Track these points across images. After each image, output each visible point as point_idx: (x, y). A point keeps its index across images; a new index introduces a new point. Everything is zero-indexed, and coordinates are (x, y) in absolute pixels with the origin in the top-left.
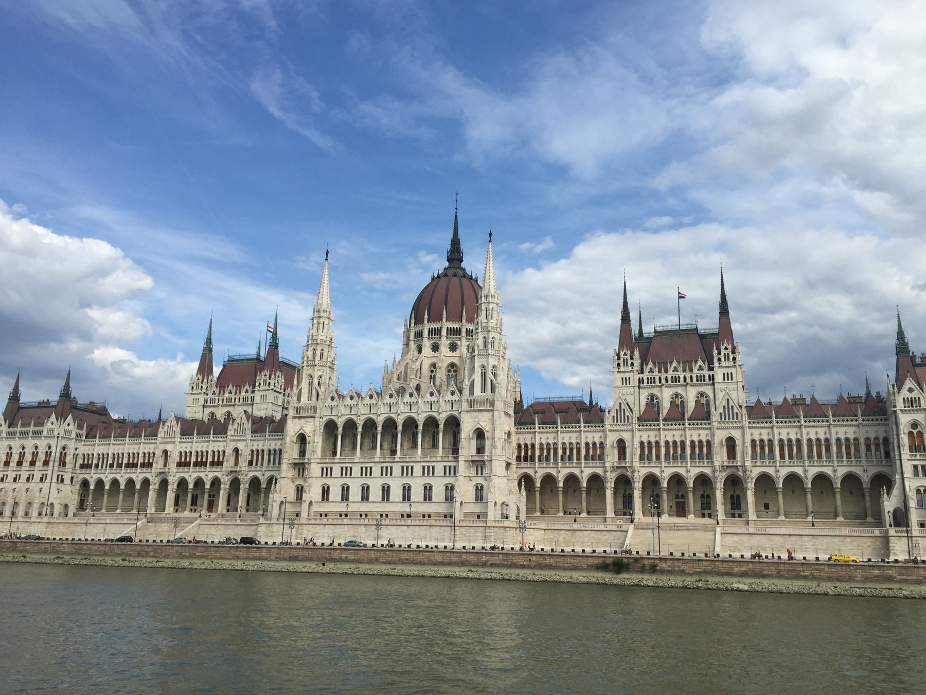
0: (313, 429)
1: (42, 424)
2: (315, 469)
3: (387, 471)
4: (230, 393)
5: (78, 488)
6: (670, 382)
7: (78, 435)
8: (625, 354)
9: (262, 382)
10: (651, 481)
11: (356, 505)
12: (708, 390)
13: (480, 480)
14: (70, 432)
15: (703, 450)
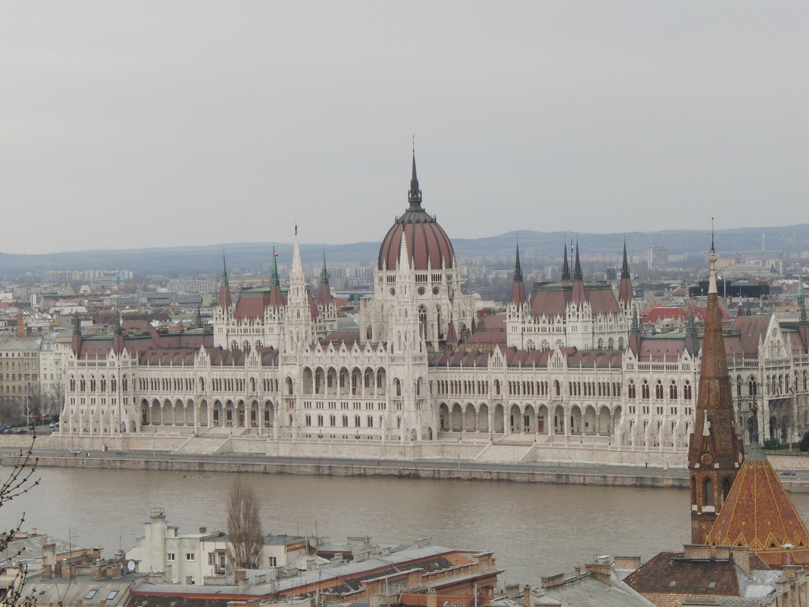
0: (295, 372)
1: (103, 356)
2: (299, 403)
3: (345, 406)
4: (246, 324)
5: (139, 405)
6: (540, 330)
7: (133, 363)
8: (514, 308)
9: (268, 316)
10: (515, 408)
11: (327, 429)
12: (562, 338)
13: (399, 413)
14: (127, 362)
15: (542, 388)
